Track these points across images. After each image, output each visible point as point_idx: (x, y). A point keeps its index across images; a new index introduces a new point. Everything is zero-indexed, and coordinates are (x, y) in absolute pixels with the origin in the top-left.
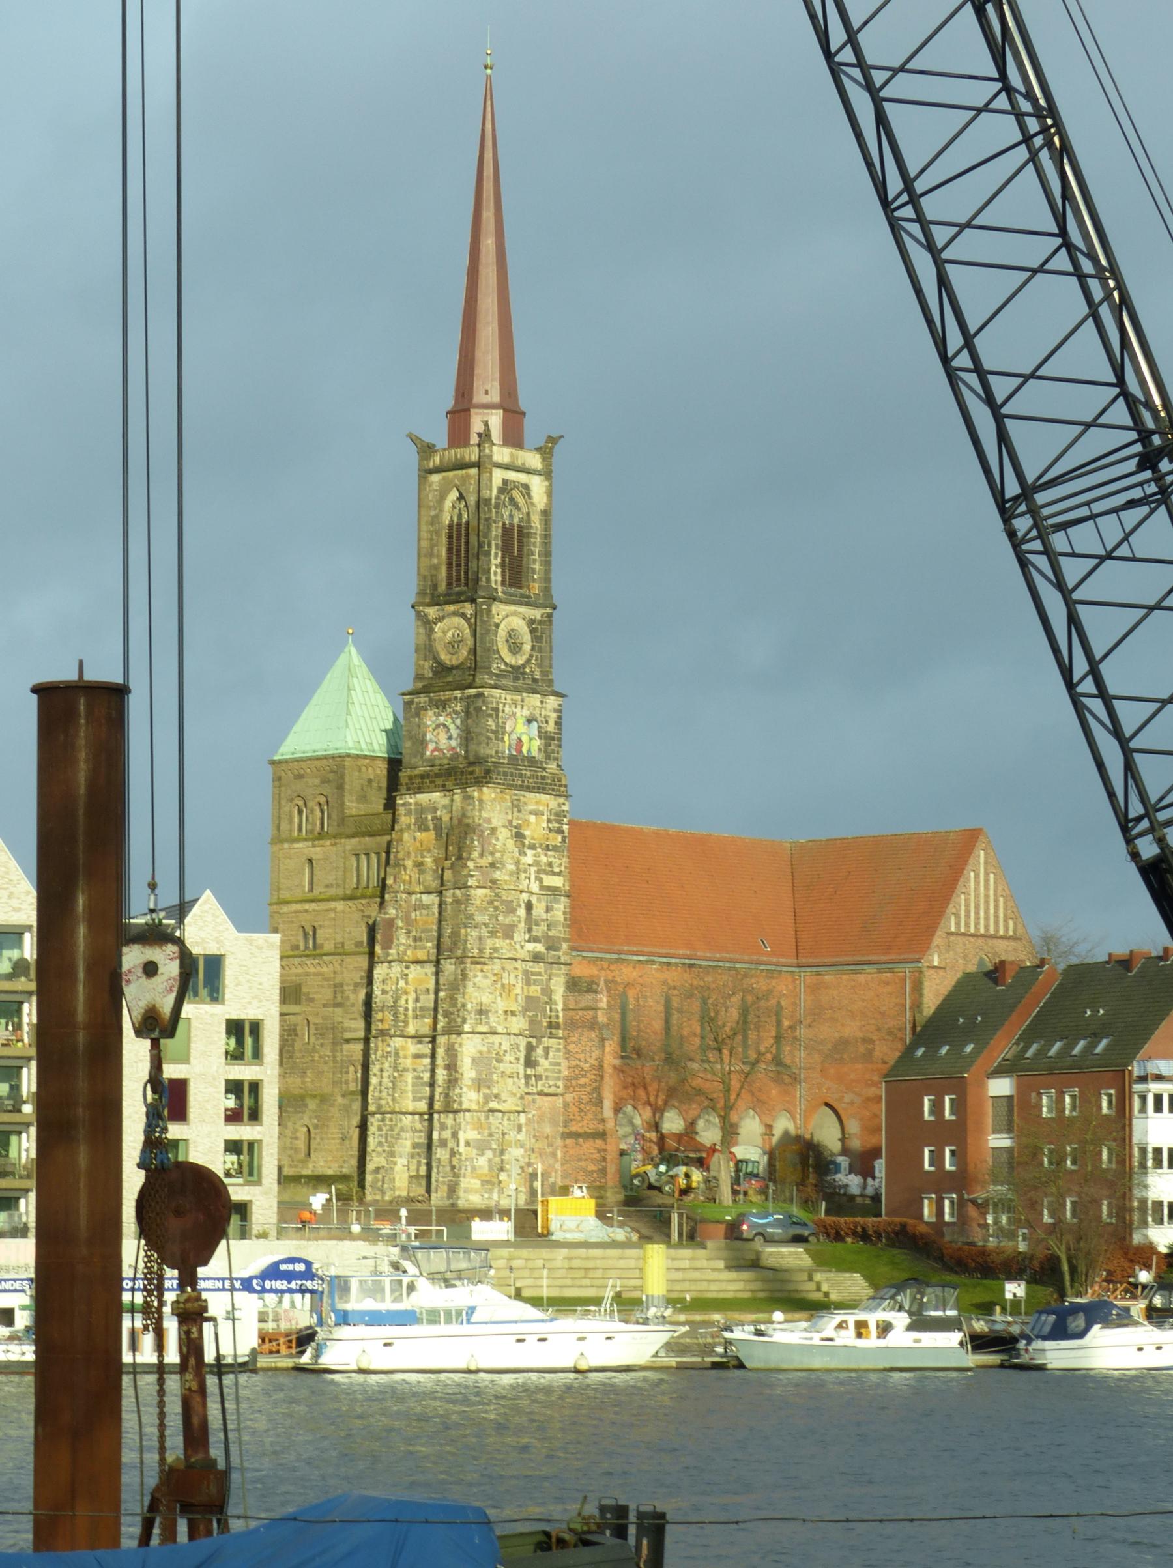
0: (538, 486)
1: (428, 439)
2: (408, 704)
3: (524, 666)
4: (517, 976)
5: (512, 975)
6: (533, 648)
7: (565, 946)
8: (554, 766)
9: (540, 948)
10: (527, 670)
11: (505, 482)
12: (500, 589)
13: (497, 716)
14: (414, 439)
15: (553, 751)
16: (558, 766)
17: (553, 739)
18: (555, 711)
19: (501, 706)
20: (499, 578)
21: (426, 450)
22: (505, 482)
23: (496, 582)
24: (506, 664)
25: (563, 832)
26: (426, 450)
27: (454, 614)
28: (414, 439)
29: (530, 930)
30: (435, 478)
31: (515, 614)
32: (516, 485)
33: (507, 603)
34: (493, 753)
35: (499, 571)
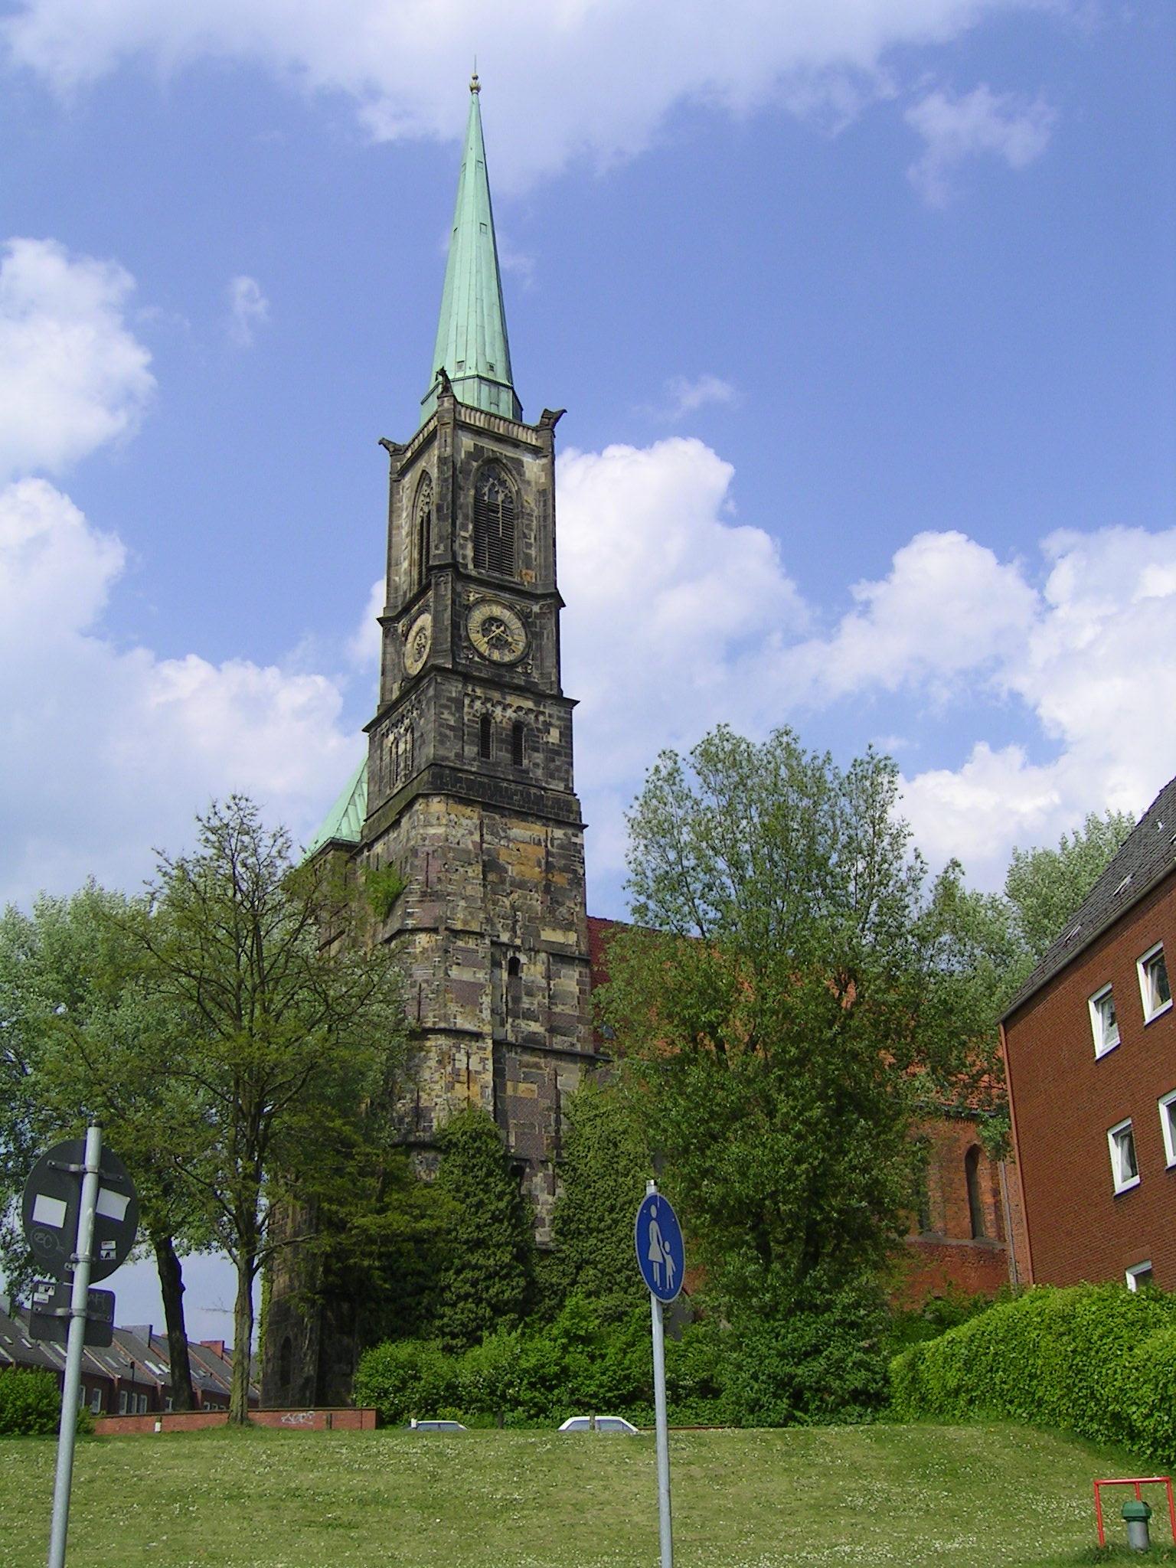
0: (532, 466)
3: (511, 666)
4: (483, 1060)
5: (474, 1060)
6: (529, 645)
7: (582, 1030)
8: (561, 787)
9: (535, 1027)
15: (558, 769)
16: (566, 787)
17: (558, 753)
18: (559, 718)
24: (481, 656)
27: (420, 613)
29: (517, 1000)
34: (452, 755)
35: (470, 545)
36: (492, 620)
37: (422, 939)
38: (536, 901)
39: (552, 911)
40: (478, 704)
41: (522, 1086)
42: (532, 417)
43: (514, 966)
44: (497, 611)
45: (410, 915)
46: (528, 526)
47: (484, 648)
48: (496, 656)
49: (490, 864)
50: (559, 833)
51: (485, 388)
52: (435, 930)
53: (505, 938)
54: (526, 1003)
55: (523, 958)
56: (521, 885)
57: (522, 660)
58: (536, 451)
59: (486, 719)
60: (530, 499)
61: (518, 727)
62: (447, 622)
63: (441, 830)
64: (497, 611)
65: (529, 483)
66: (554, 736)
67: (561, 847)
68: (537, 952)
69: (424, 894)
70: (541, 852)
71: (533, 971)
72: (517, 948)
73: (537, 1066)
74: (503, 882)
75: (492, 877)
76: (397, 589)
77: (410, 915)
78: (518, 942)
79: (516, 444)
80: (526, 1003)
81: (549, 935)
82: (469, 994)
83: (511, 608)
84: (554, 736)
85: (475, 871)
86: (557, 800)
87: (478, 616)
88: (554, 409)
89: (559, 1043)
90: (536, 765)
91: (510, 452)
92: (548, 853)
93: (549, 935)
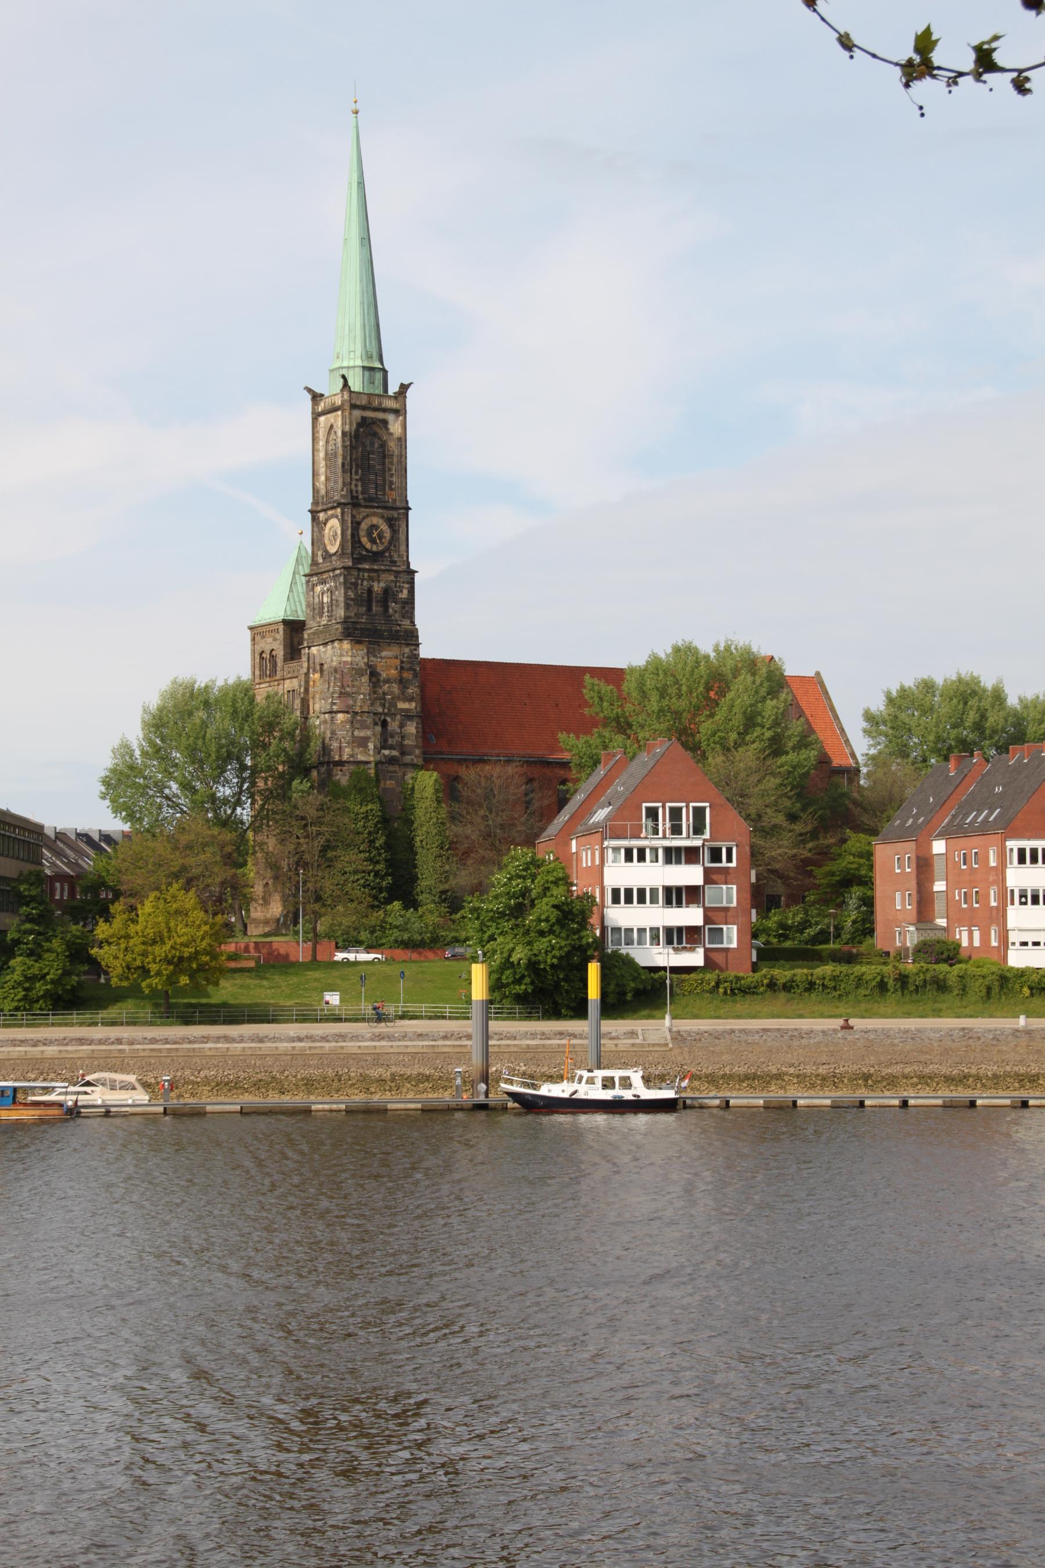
1: (318, 391)
2: (308, 582)
7: (417, 752)
9: (395, 753)
10: (387, 554)
11: (364, 419)
12: (360, 497)
13: (356, 588)
14: (309, 390)
15: (407, 612)
19: (359, 582)
20: (360, 489)
21: (316, 397)
22: (364, 419)
23: (357, 491)
24: (367, 550)
25: (415, 670)
26: (316, 397)
28: (309, 390)
29: (386, 740)
30: (322, 419)
31: (375, 514)
32: (374, 421)
33: (366, 507)
35: (360, 484)
36: (374, 527)
37: (340, 716)
38: (395, 688)
39: (403, 693)
40: (365, 583)
41: (388, 782)
42: (393, 388)
43: (384, 724)
44: (375, 520)
45: (335, 704)
46: (392, 463)
47: (368, 546)
48: (375, 548)
49: (374, 674)
50: (407, 650)
51: (367, 373)
52: (347, 712)
53: (380, 710)
54: (390, 741)
55: (389, 719)
56: (387, 681)
57: (387, 549)
58: (396, 412)
59: (370, 591)
60: (392, 445)
61: (386, 591)
62: (349, 537)
63: (349, 659)
64: (375, 520)
65: (392, 434)
66: (404, 595)
67: (408, 657)
68: (395, 715)
69: (341, 693)
70: (398, 662)
71: (394, 726)
72: (386, 714)
73: (395, 772)
74: (379, 681)
75: (374, 679)
76: (318, 491)
77: (335, 704)
78: (386, 711)
79: (385, 410)
80: (390, 741)
81: (401, 705)
82: (363, 742)
83: (383, 517)
84: (404, 595)
85: (365, 679)
86: (406, 631)
87: (364, 526)
88: (406, 383)
89: (407, 759)
90: (396, 612)
91: (380, 415)
92: (402, 662)
93: (401, 705)
